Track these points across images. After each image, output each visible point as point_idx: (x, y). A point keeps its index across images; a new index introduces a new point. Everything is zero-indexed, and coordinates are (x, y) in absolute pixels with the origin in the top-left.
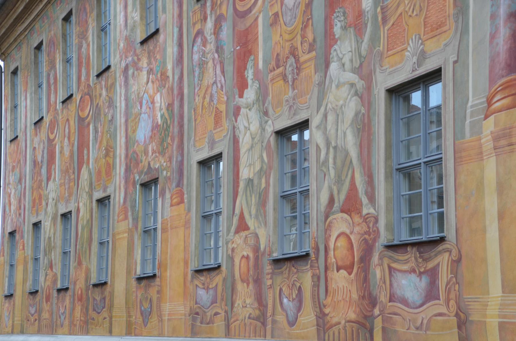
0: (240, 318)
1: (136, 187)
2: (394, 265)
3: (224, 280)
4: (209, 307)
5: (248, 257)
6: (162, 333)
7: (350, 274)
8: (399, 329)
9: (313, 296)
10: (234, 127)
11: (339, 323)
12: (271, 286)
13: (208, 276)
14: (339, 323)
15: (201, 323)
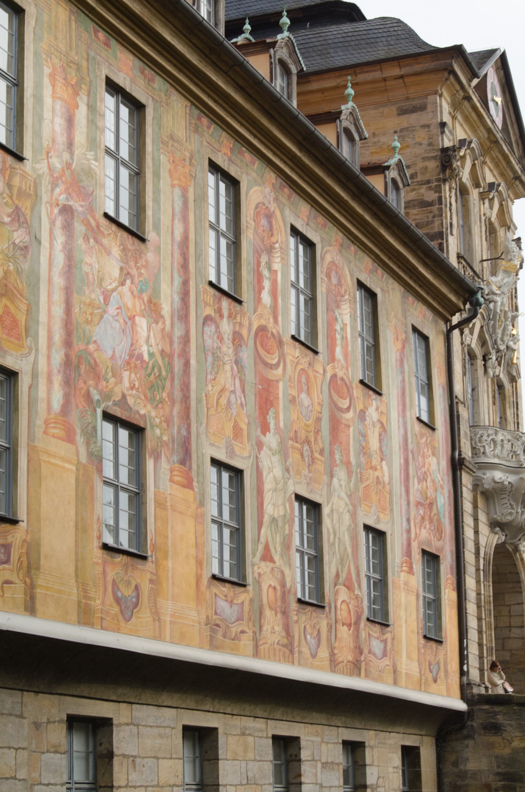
0: (269, 642)
1: (95, 411)
2: (371, 632)
3: (251, 600)
4: (234, 623)
5: (275, 588)
6: (160, 636)
7: (350, 630)
8: (372, 670)
9: (327, 638)
10: (257, 457)
11: (343, 662)
12: (297, 622)
13: (232, 590)
14: (343, 662)
15: (224, 636)
